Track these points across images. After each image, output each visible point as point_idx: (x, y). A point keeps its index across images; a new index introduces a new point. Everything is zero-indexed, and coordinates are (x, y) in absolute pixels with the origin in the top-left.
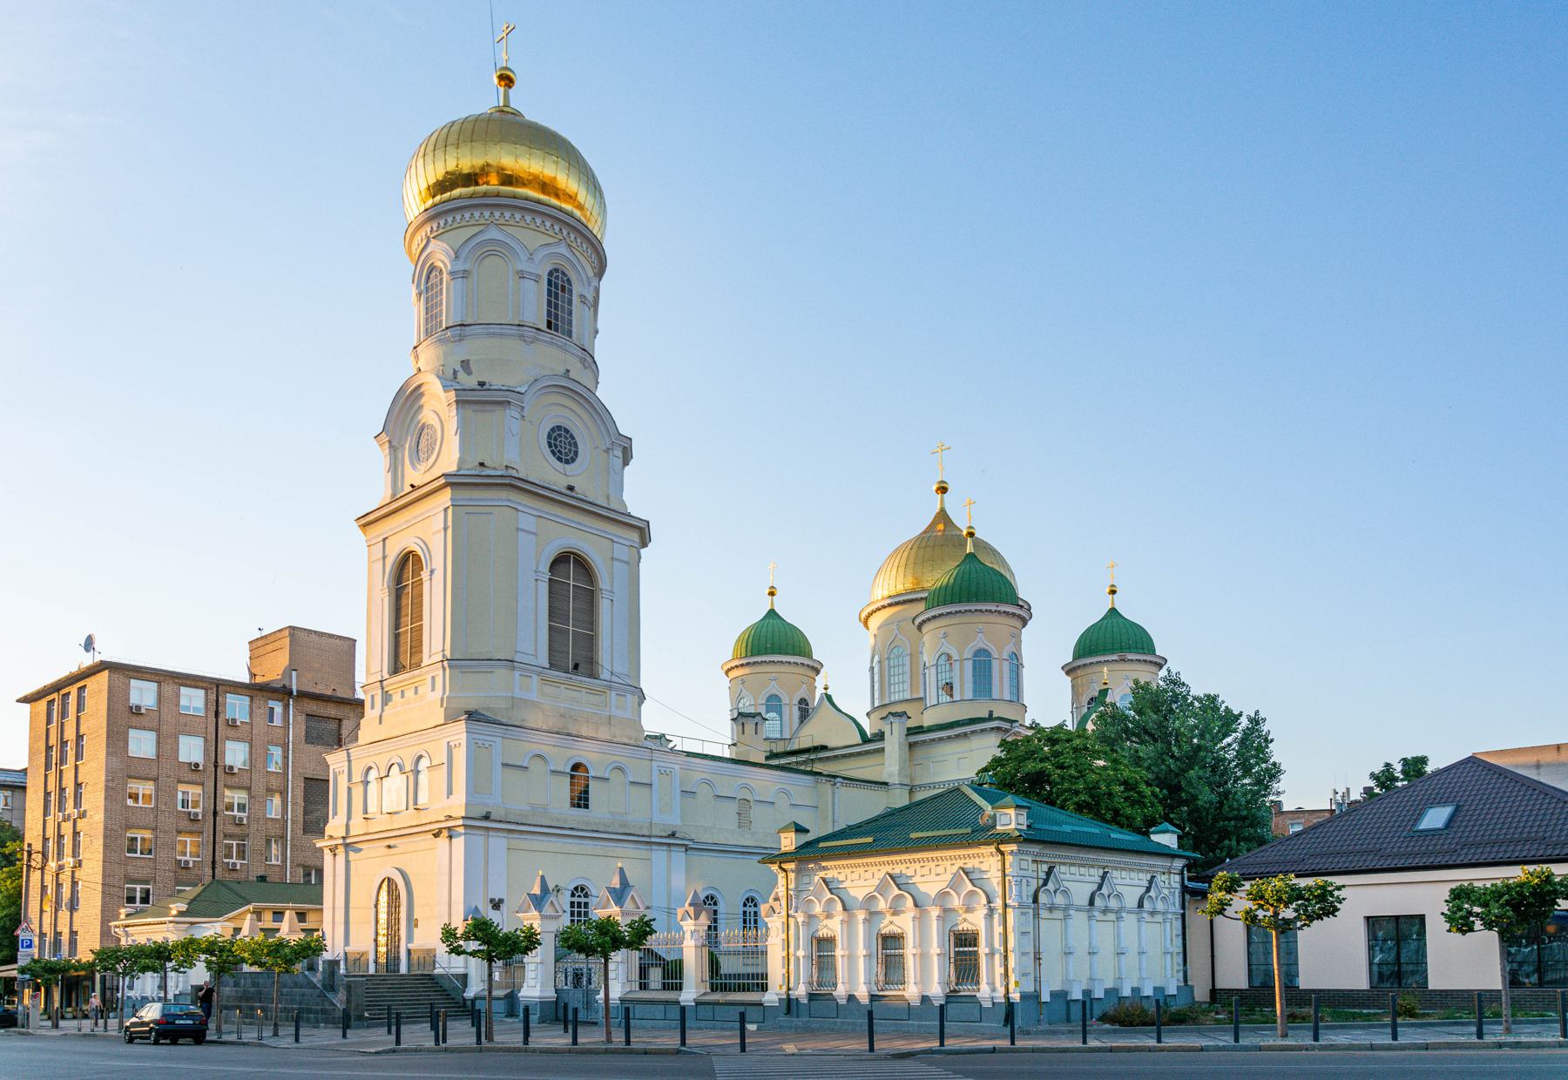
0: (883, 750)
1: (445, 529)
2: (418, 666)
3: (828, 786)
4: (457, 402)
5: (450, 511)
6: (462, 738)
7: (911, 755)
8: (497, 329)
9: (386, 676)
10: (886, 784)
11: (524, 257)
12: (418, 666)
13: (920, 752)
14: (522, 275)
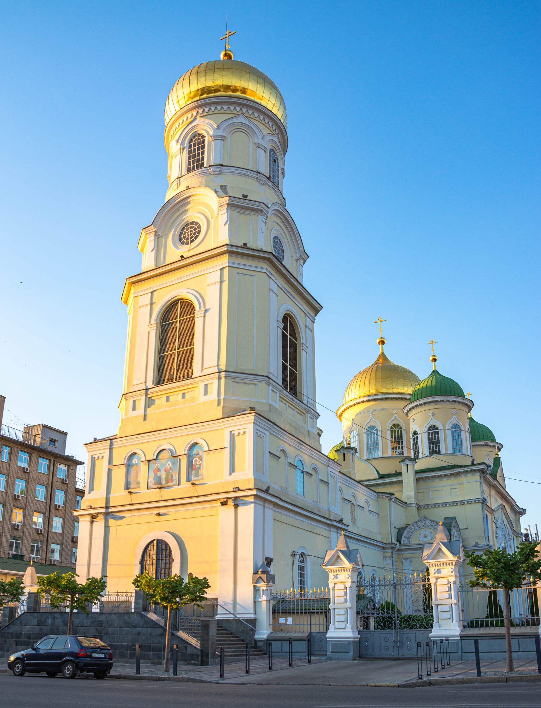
0: (401, 482)
1: (221, 282)
2: (189, 376)
3: (387, 499)
4: (228, 204)
5: (226, 271)
6: (250, 429)
7: (417, 487)
8: (244, 172)
9: (150, 384)
10: (406, 503)
11: (260, 137)
12: (189, 376)
13: (423, 484)
14: (258, 146)
